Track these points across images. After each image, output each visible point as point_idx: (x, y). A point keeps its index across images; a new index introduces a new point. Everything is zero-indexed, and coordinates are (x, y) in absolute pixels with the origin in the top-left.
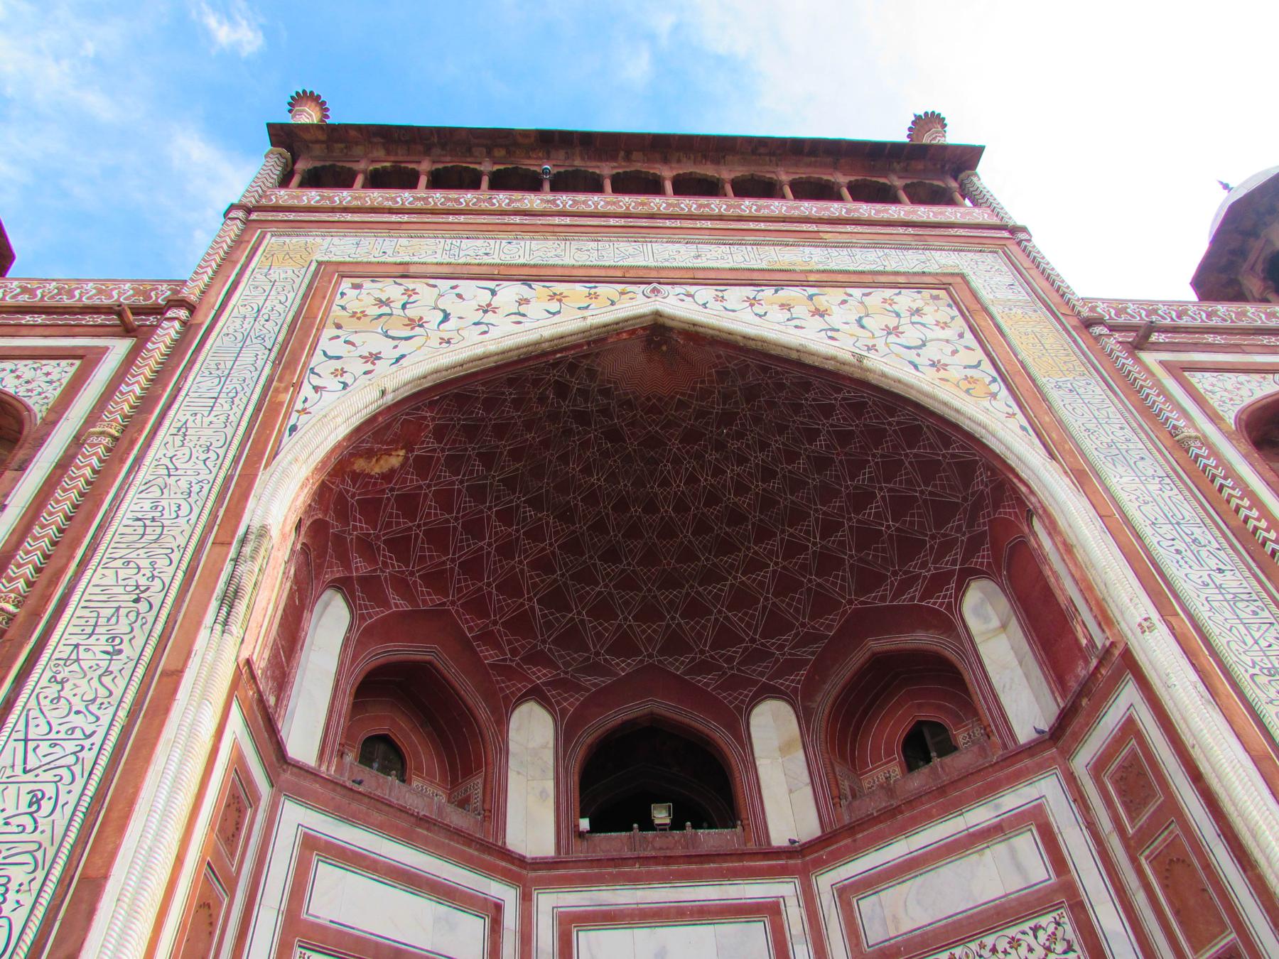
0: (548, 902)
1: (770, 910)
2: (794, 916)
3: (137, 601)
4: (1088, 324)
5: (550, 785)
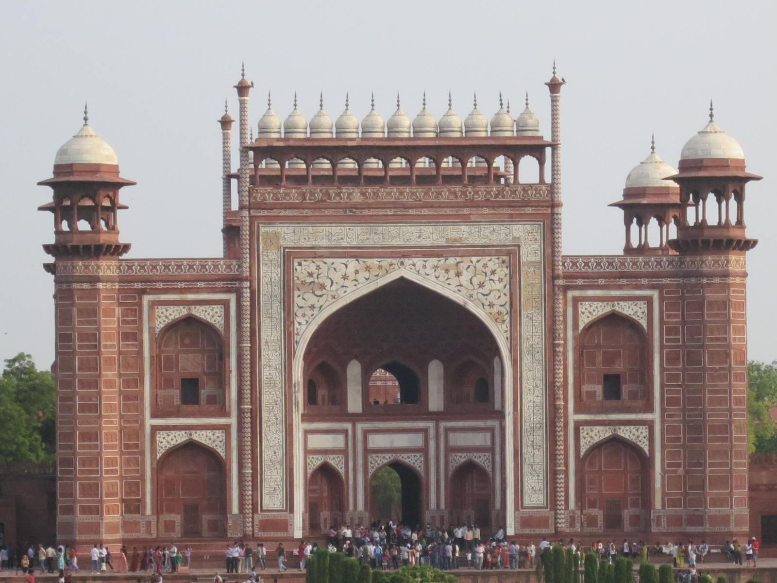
0: (361, 426)
1: (425, 431)
2: (432, 432)
3: (276, 404)
4: (554, 277)
5: (360, 388)
